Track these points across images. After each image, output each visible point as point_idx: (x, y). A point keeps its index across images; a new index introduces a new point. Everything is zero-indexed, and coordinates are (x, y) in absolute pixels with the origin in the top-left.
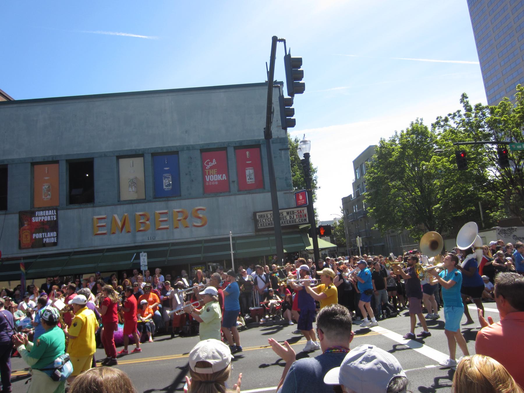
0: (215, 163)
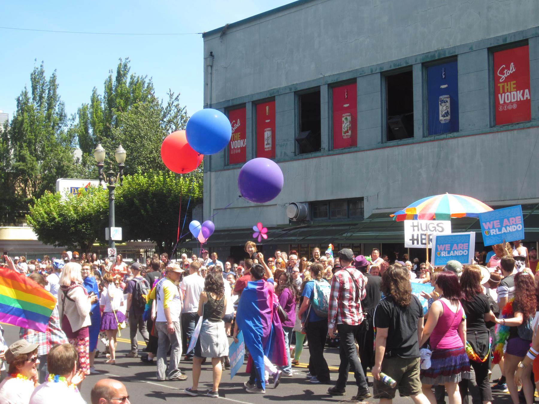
0: (514, 70)
